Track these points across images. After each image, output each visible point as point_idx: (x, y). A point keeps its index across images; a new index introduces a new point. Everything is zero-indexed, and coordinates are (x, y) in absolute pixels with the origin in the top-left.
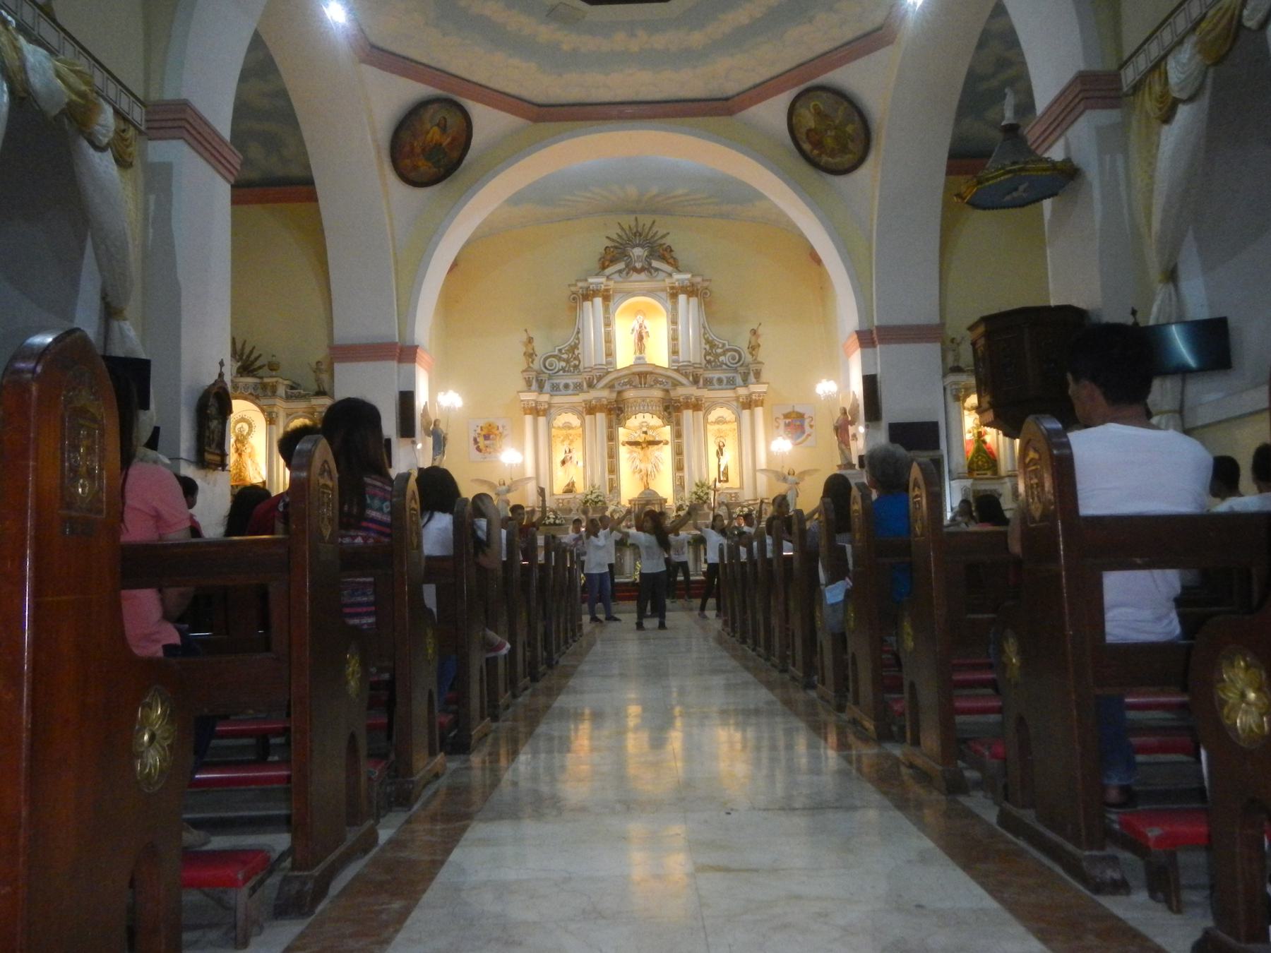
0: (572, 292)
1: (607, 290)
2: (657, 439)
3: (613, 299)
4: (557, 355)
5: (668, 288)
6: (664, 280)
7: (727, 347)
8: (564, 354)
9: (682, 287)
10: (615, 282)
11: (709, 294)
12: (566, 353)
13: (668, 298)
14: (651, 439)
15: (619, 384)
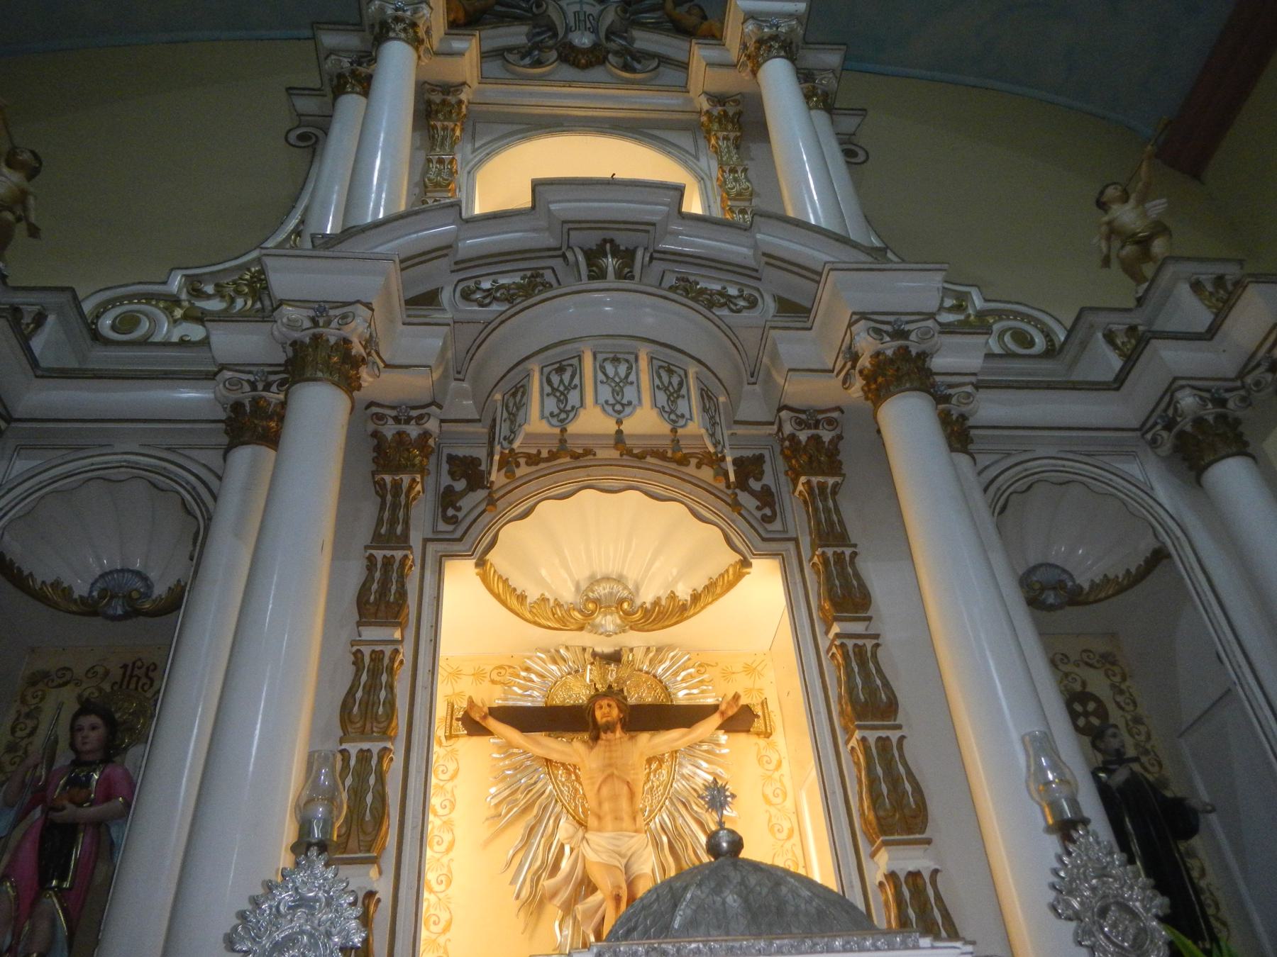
0: (299, 115)
1: (450, 89)
2: (682, 696)
3: (473, 138)
4: (175, 301)
5: (703, 100)
6: (684, 88)
7: (978, 302)
8: (209, 297)
9: (774, 38)
10: (483, 79)
11: (861, 153)
12: (219, 292)
13: (702, 142)
14: (640, 694)
15: (466, 295)
